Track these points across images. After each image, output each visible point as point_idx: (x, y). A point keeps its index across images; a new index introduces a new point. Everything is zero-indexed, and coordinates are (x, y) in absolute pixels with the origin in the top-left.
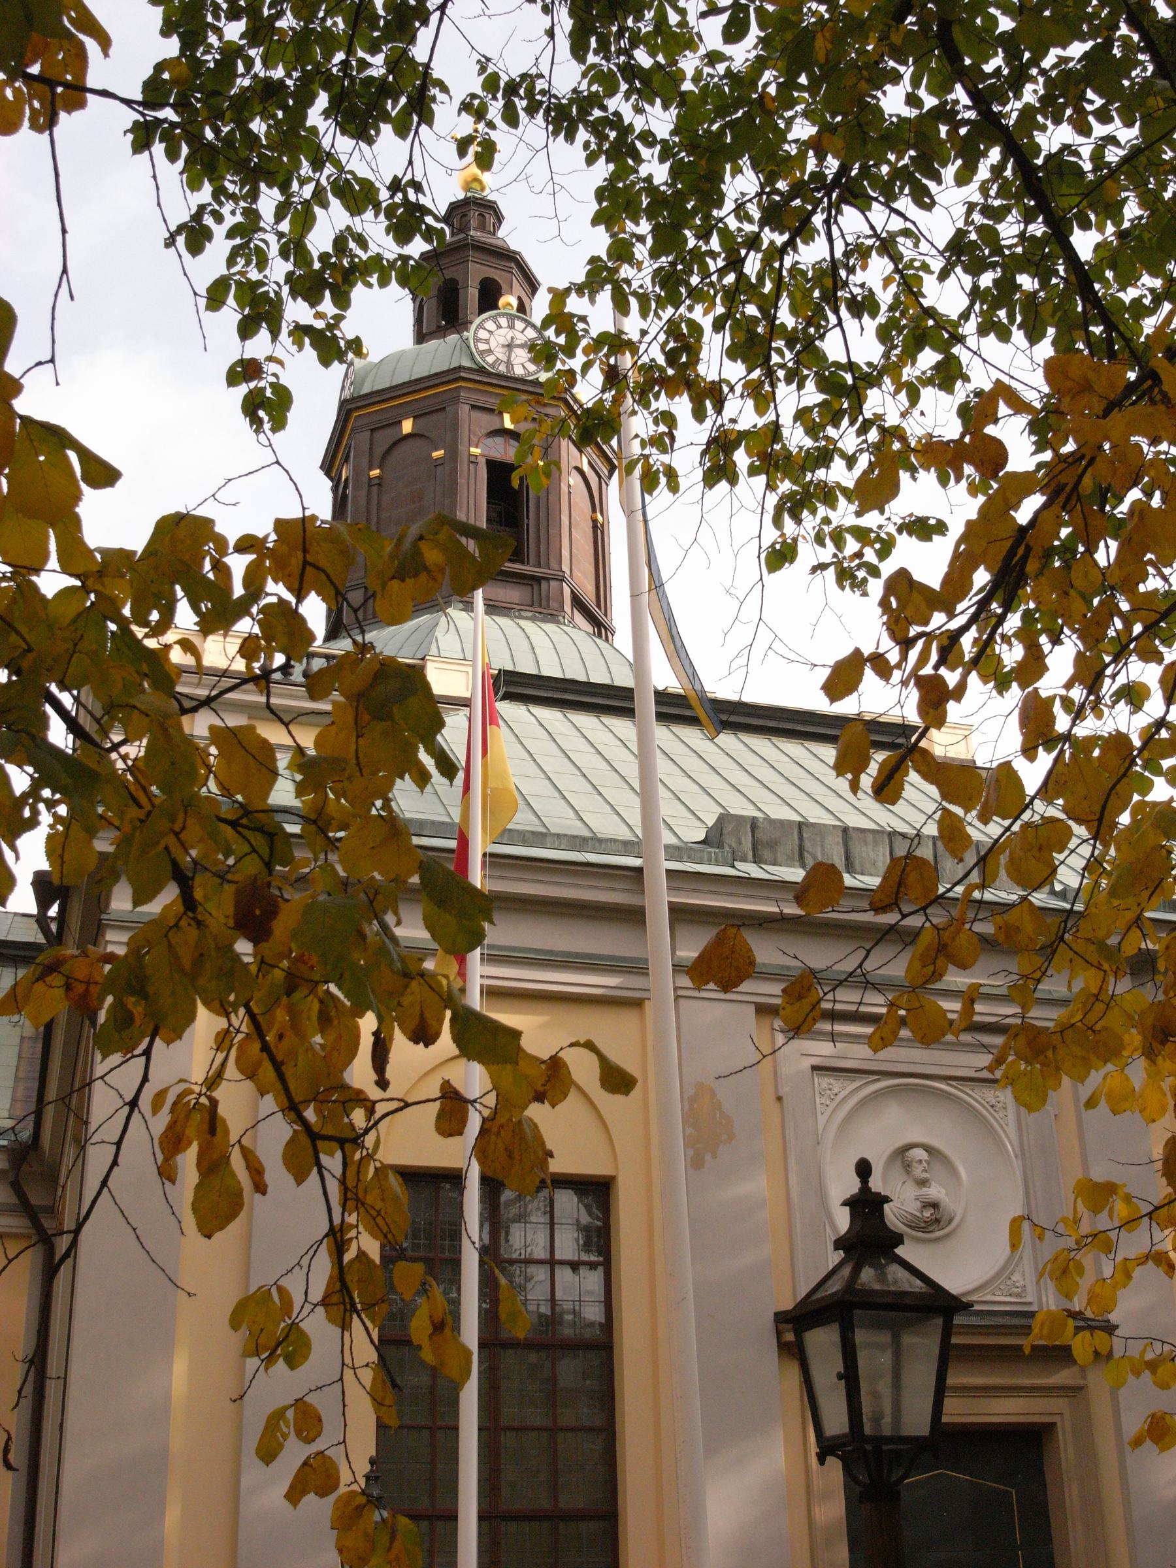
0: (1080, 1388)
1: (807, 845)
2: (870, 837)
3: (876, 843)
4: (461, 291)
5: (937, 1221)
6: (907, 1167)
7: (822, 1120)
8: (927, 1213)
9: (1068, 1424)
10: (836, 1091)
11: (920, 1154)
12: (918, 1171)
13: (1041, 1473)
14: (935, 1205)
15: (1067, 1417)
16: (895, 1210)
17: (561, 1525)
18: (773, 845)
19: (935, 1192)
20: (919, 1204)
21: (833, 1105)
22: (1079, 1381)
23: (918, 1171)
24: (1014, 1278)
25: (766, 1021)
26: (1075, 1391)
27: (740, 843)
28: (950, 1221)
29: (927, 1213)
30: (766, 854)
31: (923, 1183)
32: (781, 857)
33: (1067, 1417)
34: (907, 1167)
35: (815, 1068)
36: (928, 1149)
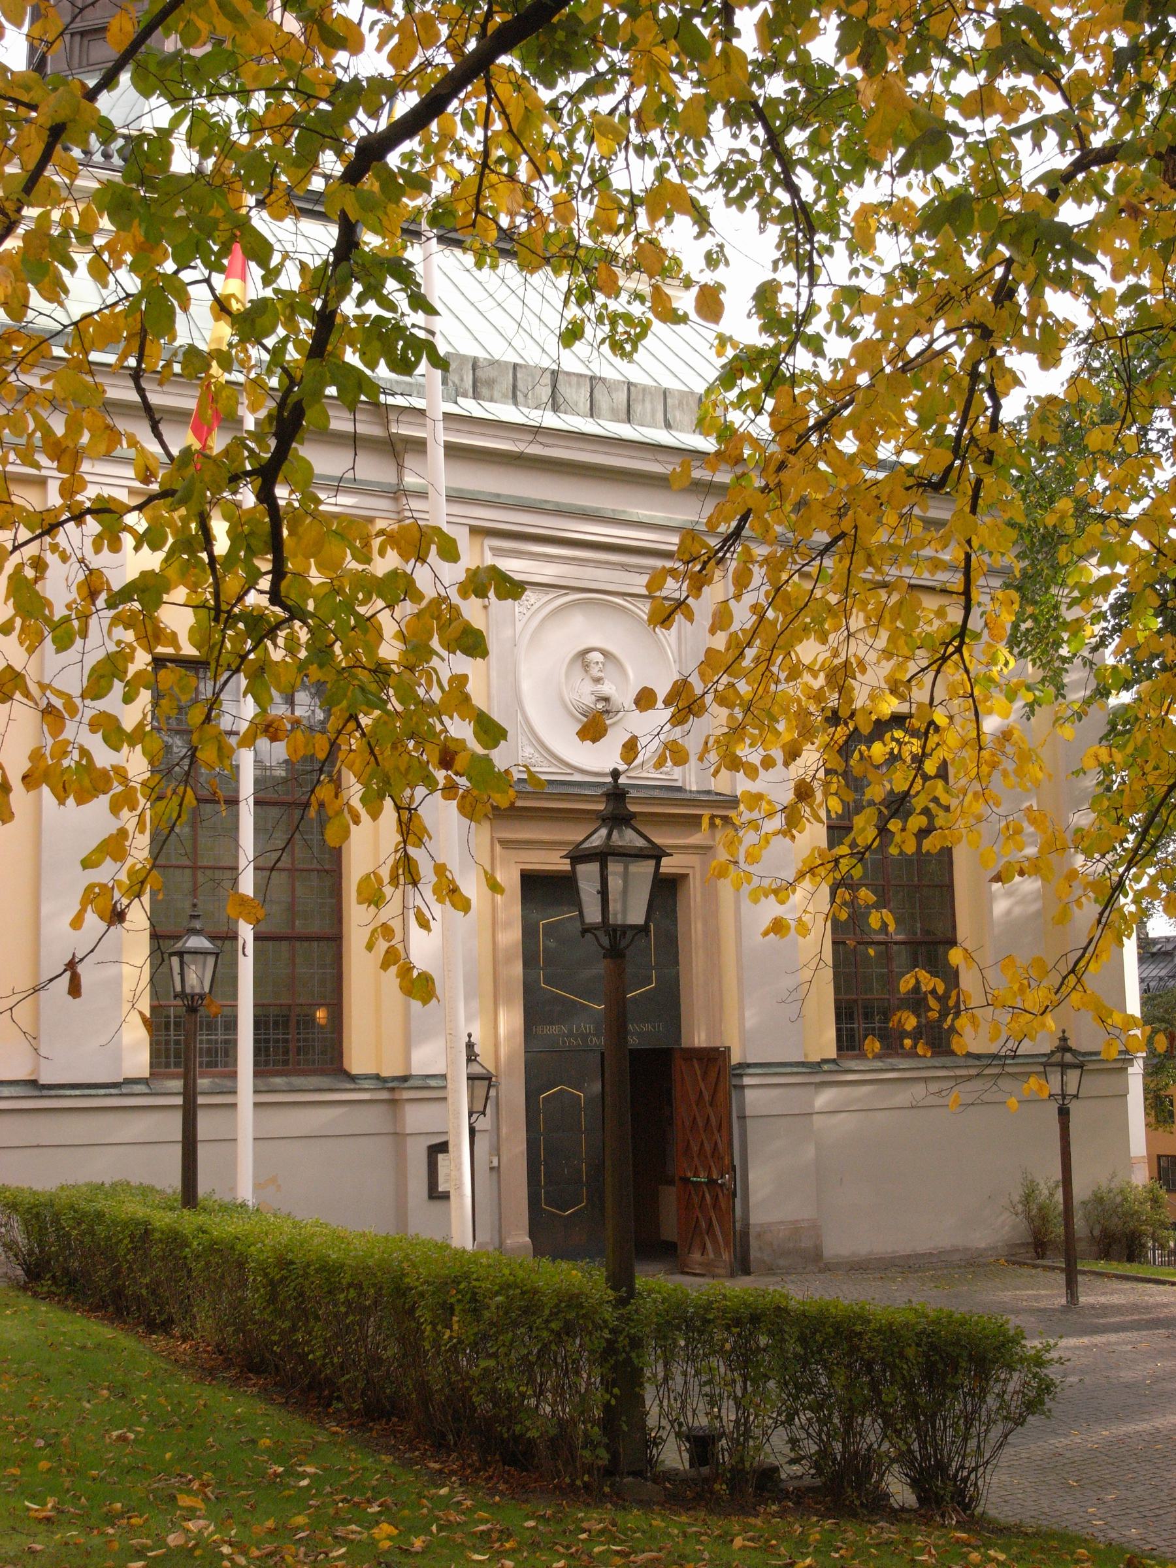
1: (520, 384)
2: (574, 380)
3: (579, 384)
5: (607, 712)
6: (586, 667)
7: (519, 626)
9: (698, 876)
11: (596, 656)
12: (595, 671)
13: (674, 911)
14: (606, 700)
15: (698, 869)
17: (298, 944)
18: (491, 383)
19: (607, 689)
21: (528, 614)
22: (710, 843)
23: (595, 671)
25: (478, 540)
26: (705, 850)
27: (462, 380)
29: (600, 706)
30: (484, 391)
31: (597, 680)
32: (496, 395)
33: (698, 869)
34: (586, 667)
36: (604, 653)
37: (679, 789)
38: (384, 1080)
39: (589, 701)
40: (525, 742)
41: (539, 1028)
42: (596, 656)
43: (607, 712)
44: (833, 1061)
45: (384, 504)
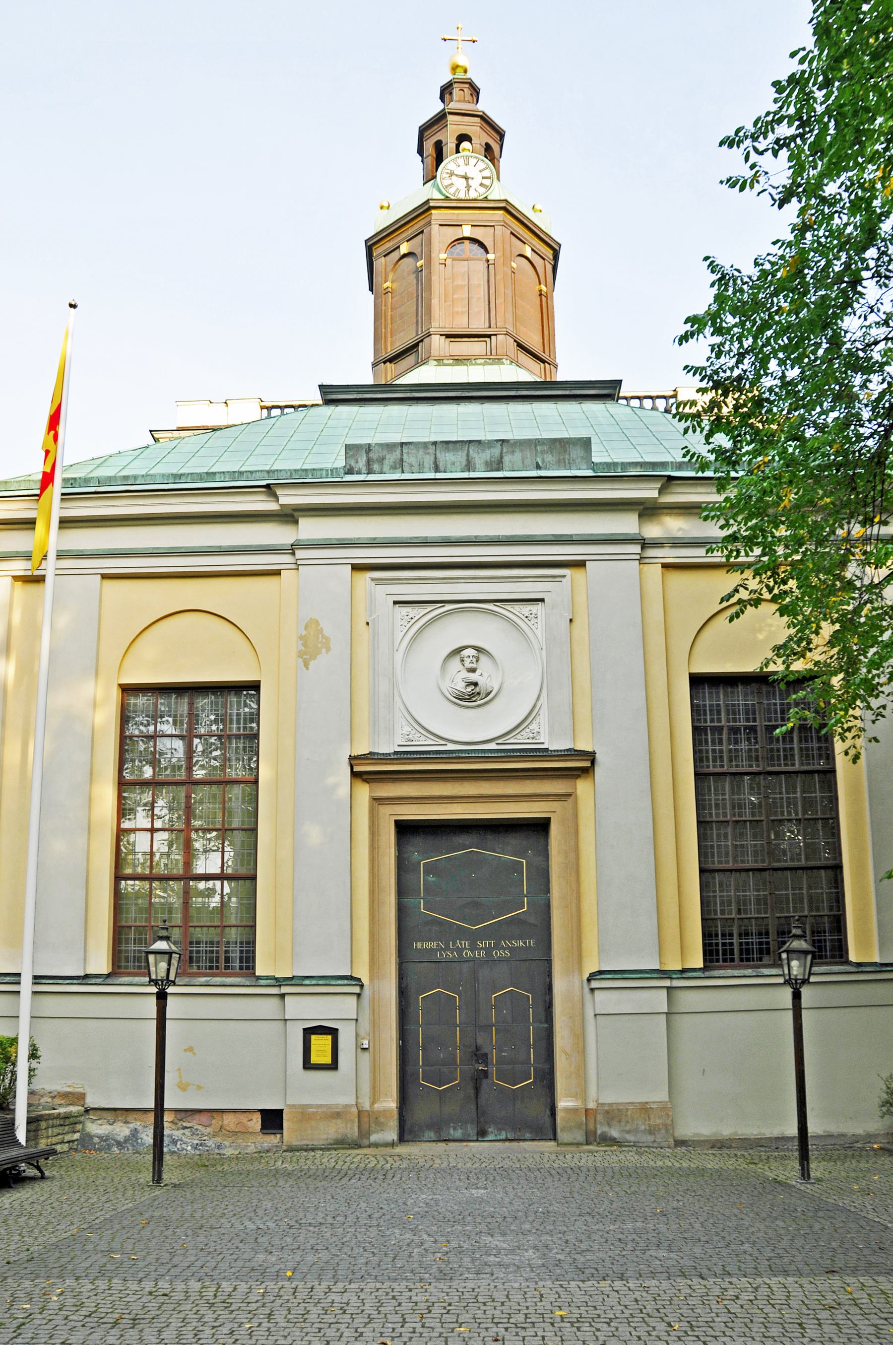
0: (570, 795)
4: (444, 148)
8: (469, 689)
10: (411, 615)
11: (470, 652)
14: (476, 684)
16: (450, 689)
19: (473, 677)
20: (464, 684)
22: (569, 791)
24: (531, 727)
28: (488, 694)
29: (469, 689)
31: (473, 670)
35: (395, 603)
36: (478, 649)
37: (546, 750)
38: (276, 979)
39: (461, 686)
40: (404, 722)
41: (419, 945)
42: (466, 653)
43: (479, 694)
44: (700, 969)
45: (288, 558)
